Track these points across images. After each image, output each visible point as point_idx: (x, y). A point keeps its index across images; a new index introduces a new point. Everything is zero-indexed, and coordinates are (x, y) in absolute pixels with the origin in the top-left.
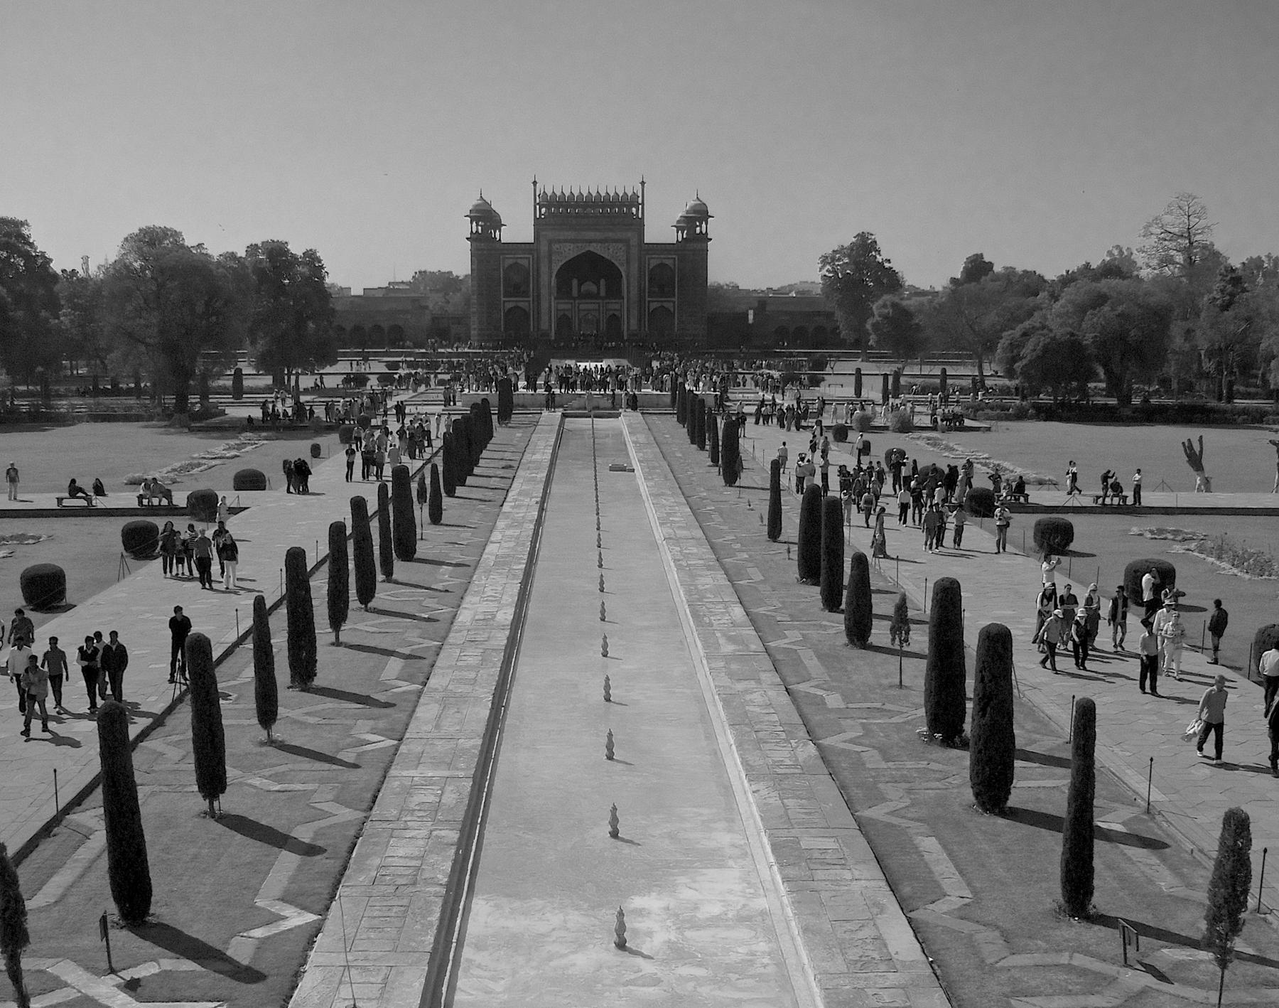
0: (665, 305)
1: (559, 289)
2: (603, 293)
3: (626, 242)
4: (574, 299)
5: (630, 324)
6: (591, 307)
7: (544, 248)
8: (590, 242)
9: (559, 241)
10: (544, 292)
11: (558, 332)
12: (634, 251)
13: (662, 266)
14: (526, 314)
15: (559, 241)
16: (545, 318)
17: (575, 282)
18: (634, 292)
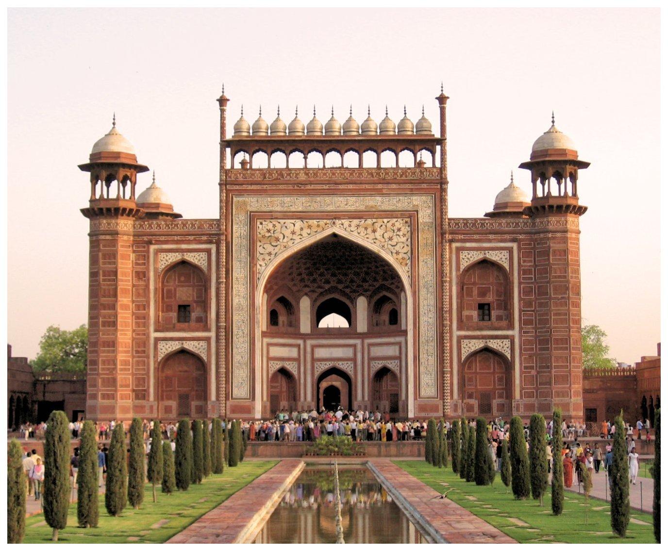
0: (494, 344)
1: (273, 317)
2: (362, 326)
3: (411, 217)
4: (305, 337)
6: (338, 353)
7: (239, 230)
8: (335, 216)
9: (270, 216)
10: (239, 319)
12: (427, 237)
15: (270, 216)
16: (240, 375)
17: (305, 306)
18: (428, 319)
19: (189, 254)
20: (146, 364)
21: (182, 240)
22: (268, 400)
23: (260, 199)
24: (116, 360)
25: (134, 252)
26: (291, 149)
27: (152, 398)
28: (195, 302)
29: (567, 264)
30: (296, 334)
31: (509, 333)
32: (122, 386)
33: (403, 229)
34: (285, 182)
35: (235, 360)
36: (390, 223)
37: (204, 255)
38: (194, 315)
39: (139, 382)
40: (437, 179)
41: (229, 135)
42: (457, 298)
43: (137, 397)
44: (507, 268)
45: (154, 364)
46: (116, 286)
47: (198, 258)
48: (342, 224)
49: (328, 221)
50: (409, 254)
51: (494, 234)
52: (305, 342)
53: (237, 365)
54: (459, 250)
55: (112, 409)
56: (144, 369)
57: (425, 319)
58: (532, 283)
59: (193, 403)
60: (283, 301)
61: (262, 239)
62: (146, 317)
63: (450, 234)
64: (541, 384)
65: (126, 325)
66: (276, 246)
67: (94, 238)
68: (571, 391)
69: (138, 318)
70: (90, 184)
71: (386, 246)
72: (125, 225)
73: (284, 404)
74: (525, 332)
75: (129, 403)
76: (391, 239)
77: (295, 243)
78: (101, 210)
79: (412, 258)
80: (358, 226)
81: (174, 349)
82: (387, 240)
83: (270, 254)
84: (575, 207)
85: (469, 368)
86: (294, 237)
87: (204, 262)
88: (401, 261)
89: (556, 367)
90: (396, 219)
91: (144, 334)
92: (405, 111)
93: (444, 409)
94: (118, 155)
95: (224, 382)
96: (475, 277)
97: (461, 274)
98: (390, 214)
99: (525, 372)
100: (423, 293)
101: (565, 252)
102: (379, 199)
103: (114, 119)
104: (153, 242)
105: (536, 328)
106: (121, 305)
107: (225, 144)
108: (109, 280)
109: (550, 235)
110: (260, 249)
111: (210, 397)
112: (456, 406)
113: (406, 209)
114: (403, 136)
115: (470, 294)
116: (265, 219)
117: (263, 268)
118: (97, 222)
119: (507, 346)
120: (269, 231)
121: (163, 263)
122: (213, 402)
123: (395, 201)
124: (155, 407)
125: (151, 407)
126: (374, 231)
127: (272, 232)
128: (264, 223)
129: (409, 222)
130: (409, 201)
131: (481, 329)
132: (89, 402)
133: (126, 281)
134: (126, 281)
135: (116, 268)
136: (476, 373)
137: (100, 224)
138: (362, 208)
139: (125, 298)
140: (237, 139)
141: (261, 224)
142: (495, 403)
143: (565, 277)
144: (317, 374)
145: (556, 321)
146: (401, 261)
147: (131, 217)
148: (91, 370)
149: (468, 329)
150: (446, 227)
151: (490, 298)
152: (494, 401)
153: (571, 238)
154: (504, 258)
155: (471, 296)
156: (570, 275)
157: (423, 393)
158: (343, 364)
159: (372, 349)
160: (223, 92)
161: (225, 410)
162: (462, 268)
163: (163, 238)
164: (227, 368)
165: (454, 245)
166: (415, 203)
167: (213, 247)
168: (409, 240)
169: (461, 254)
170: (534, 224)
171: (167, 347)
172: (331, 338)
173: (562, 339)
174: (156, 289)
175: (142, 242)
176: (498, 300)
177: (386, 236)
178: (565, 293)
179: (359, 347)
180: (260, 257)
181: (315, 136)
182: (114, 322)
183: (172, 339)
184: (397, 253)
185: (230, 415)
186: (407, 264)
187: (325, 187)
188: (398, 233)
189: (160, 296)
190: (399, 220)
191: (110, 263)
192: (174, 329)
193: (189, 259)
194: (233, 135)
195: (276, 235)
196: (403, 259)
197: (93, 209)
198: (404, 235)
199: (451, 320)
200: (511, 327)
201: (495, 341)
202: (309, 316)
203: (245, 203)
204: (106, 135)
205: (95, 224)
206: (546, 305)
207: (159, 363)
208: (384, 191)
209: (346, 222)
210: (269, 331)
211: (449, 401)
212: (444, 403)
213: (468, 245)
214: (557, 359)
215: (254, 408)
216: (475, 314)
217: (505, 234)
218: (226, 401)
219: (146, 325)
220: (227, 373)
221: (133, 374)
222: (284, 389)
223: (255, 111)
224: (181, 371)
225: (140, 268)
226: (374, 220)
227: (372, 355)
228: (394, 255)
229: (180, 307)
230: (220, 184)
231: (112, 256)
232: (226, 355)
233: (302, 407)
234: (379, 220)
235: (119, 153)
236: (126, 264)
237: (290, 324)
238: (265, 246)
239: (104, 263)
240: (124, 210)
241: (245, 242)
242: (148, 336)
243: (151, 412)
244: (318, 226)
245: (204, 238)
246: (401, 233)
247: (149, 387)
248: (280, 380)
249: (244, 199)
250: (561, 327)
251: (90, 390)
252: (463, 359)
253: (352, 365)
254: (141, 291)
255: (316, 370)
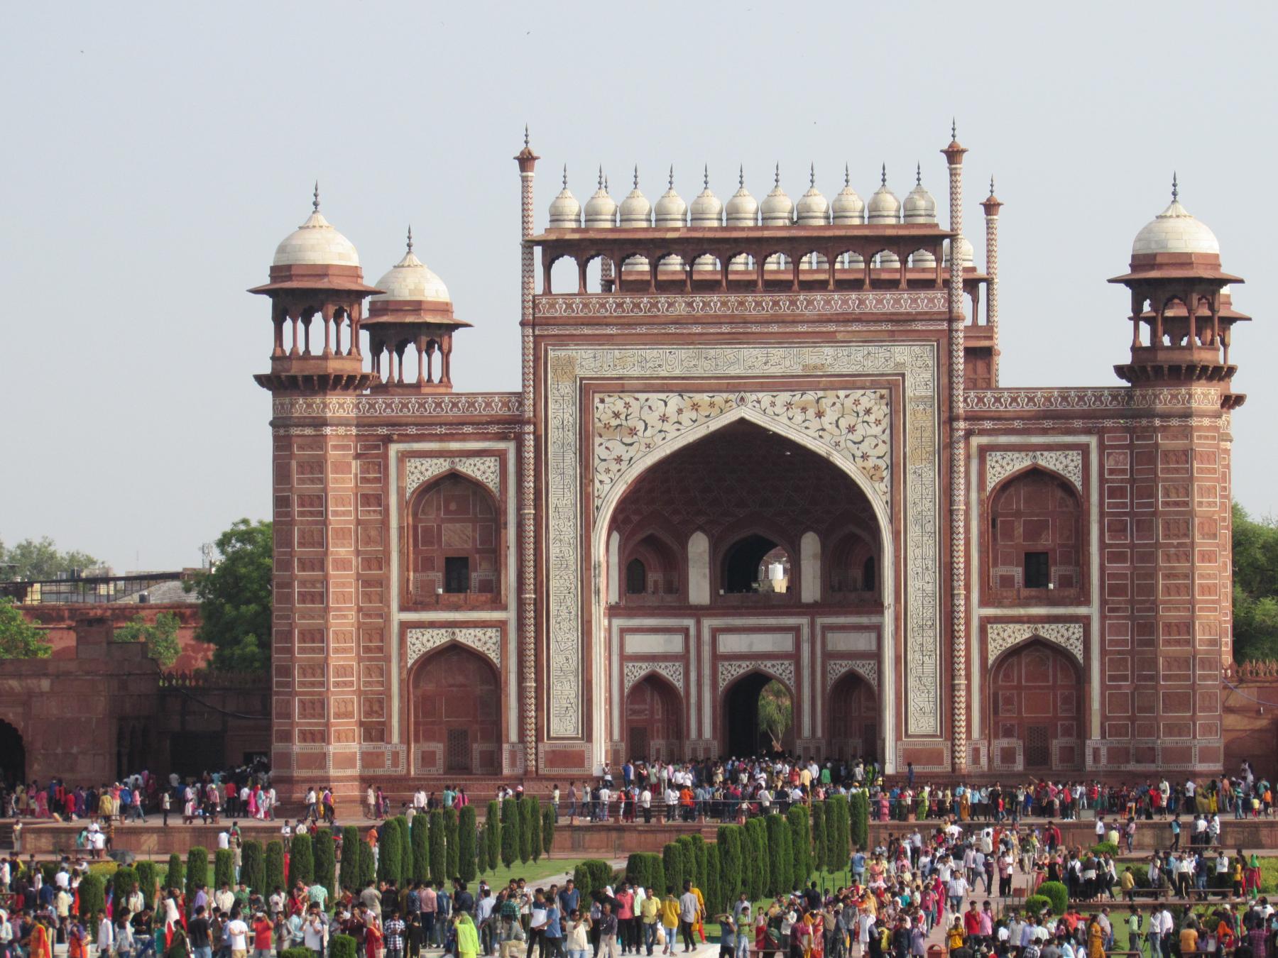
0: (1051, 633)
2: (811, 591)
5: (912, 711)
6: (763, 643)
7: (561, 414)
9: (619, 386)
10: (562, 583)
11: (635, 744)
12: (921, 422)
13: (1035, 475)
14: (489, 672)
15: (619, 386)
16: (563, 691)
17: (699, 546)
19: (464, 459)
20: (384, 673)
21: (452, 434)
22: (622, 739)
23: (599, 353)
24: (327, 629)
25: (358, 456)
26: (659, 254)
27: (395, 738)
28: (478, 551)
29: (1191, 479)
30: (680, 608)
31: (1082, 611)
32: (338, 716)
33: (875, 409)
34: (647, 321)
35: (553, 665)
36: (851, 400)
37: (491, 463)
38: (475, 577)
39: (371, 707)
40: (940, 313)
41: (539, 228)
42: (981, 545)
43: (368, 737)
44: (1078, 485)
45: (400, 673)
46: (325, 523)
47: (482, 468)
48: (759, 402)
49: (732, 396)
50: (887, 459)
51: (1053, 418)
52: (698, 623)
53: (559, 673)
54: (983, 451)
55: (321, 760)
56: (382, 684)
57: (919, 584)
58: (1125, 514)
59: (475, 746)
60: (651, 541)
61: (603, 431)
62: (383, 583)
63: (966, 419)
64: (1141, 710)
65: (344, 597)
66: (631, 444)
67: (282, 432)
68: (1195, 725)
69: (367, 583)
70: (272, 324)
71: (842, 444)
72: (340, 405)
73: (657, 744)
74: (1111, 610)
75: (354, 747)
76: (851, 429)
77: (668, 438)
78: (294, 378)
79: (892, 467)
80: (789, 405)
81: (438, 643)
82: (845, 431)
83: (619, 460)
84: (1205, 368)
85: (1007, 677)
86: (666, 426)
87: (493, 477)
88: (872, 472)
89: (1166, 678)
90: (862, 392)
91: (381, 616)
92: (884, 175)
93: (953, 758)
94: (323, 271)
95: (533, 707)
96: (1018, 503)
97: (988, 498)
98: (850, 382)
99: (1110, 687)
100: (914, 533)
101: (1186, 455)
102: (828, 351)
103: (316, 195)
104: (395, 437)
105: (1132, 602)
106: (335, 560)
107: (528, 245)
108: (312, 514)
109: (1157, 422)
110: (600, 451)
111: (507, 736)
112: (976, 751)
113: (881, 370)
114: (877, 226)
115: (1008, 534)
116: (610, 391)
117: (607, 487)
118: (287, 400)
119: (1077, 636)
120: (617, 415)
121: (412, 477)
122: (513, 744)
123: (860, 355)
124: (403, 756)
125: (395, 755)
126: (820, 415)
127: (623, 417)
128: (607, 399)
129: (887, 396)
130: (888, 354)
131: (1026, 603)
132: (277, 747)
133: (344, 513)
134: (344, 513)
135: (325, 490)
136: (1019, 687)
137: (292, 405)
138: (798, 370)
139: (343, 546)
140: (553, 237)
141: (602, 401)
142: (1056, 744)
143: (1186, 504)
144: (722, 685)
145: (1168, 590)
146: (872, 472)
147: (350, 391)
148: (279, 684)
149: (1000, 605)
150: (961, 408)
151: (1046, 542)
152: (1055, 742)
153: (1200, 428)
154: (1072, 464)
155: (1011, 537)
156: (1197, 500)
157: (911, 730)
158: (773, 666)
159: (829, 635)
160: (526, 142)
161: (536, 761)
162: (990, 485)
163: (412, 431)
164: (538, 680)
165: (976, 441)
166: (900, 359)
167: (510, 447)
168: (888, 431)
169: (988, 458)
170: (1131, 397)
171: (425, 639)
172: (749, 615)
173: (1177, 625)
174: (401, 528)
175: (374, 440)
176: (1061, 546)
177: (843, 423)
178: (1186, 535)
179: (806, 632)
180: (601, 467)
181: (704, 229)
182: (321, 594)
183: (433, 625)
184: (865, 457)
185: (543, 770)
186: (882, 479)
187: (725, 329)
188: (866, 418)
189: (411, 541)
190: (868, 392)
191: (312, 481)
192: (436, 604)
193: (464, 470)
194: (548, 225)
195: (631, 423)
196: (876, 468)
197: (279, 377)
198: (878, 422)
199: (968, 587)
200: (1087, 602)
201: (1054, 626)
202: (707, 571)
203: (571, 361)
204: (301, 228)
205: (282, 405)
206: (1149, 557)
207: (411, 668)
208: (839, 337)
209: (765, 398)
210: (623, 603)
211: (963, 742)
212: (953, 745)
213: (1003, 440)
214: (1172, 661)
215: (591, 758)
216: (1018, 572)
217: (1073, 418)
218: (536, 742)
219: (384, 599)
220: (538, 689)
221: (360, 693)
222: (659, 716)
223: (584, 191)
224: (451, 686)
225: (370, 488)
226: (820, 394)
227: (830, 647)
228: (859, 460)
229: (447, 559)
230: (523, 324)
231: (317, 466)
232: (536, 656)
233: (694, 750)
234: (829, 393)
235: (327, 267)
236: (343, 482)
237: (670, 589)
238: (609, 444)
239: (302, 481)
240: (338, 378)
241: (571, 437)
242: (387, 617)
243: (395, 764)
244: (712, 405)
245: (494, 429)
246: (871, 418)
247: (390, 717)
248: (648, 700)
249: (570, 352)
250: (1177, 602)
251: (277, 724)
252: (990, 662)
253: (792, 668)
254: (373, 533)
255: (720, 677)
